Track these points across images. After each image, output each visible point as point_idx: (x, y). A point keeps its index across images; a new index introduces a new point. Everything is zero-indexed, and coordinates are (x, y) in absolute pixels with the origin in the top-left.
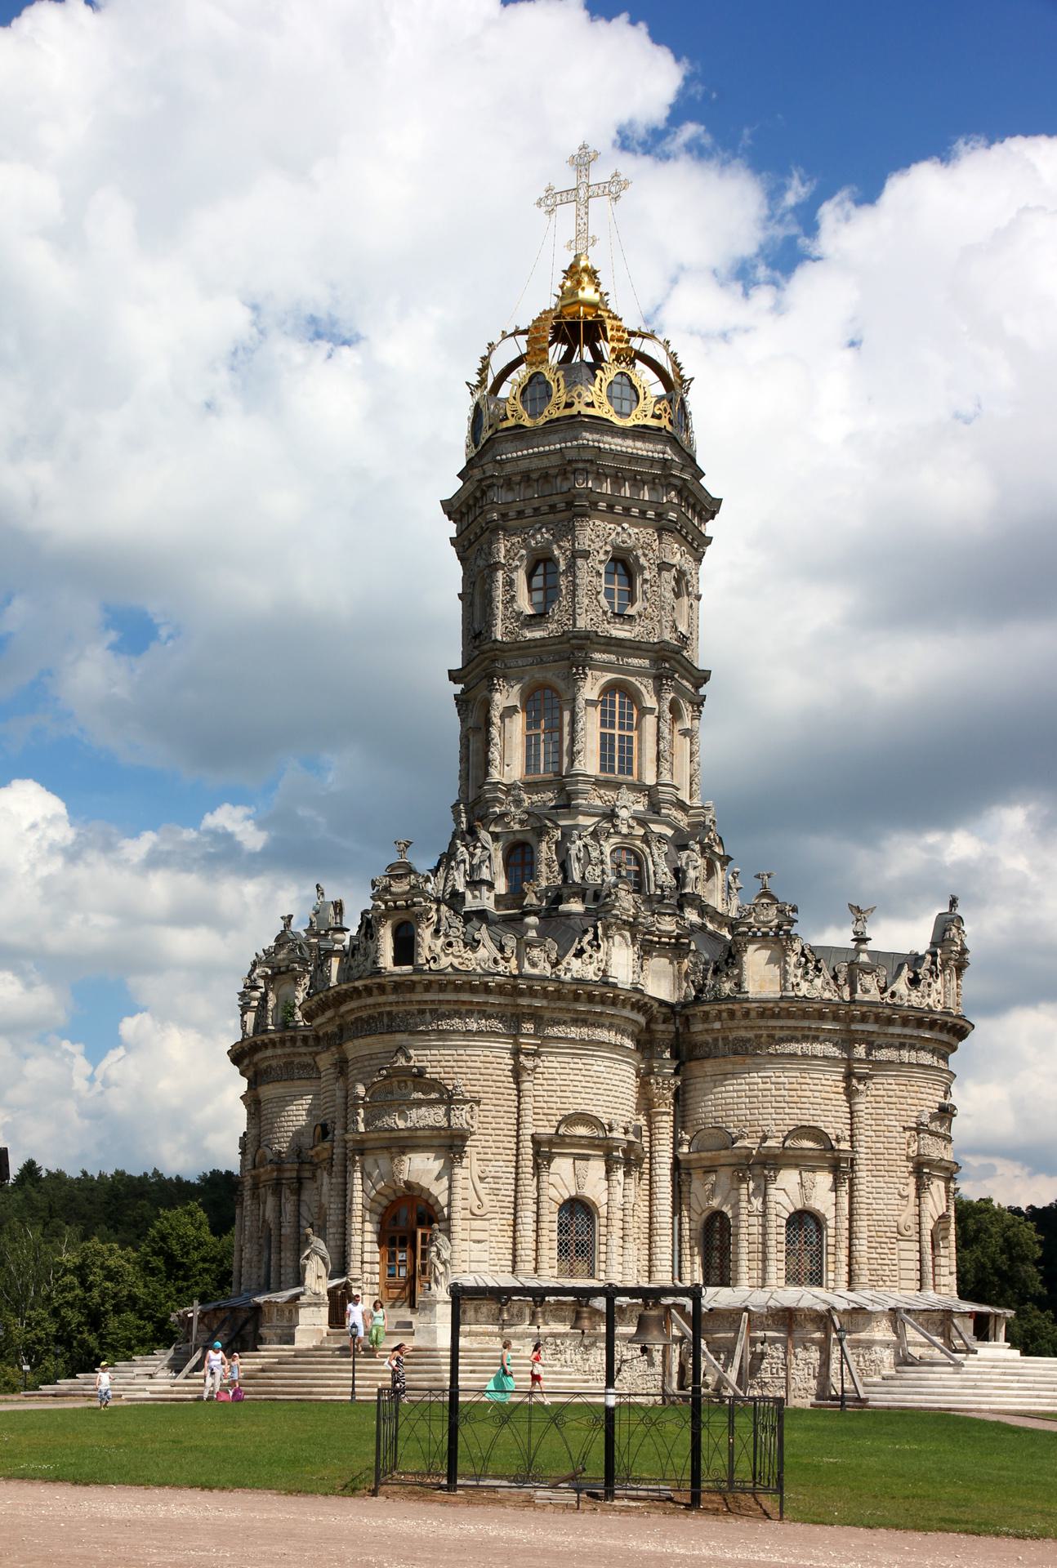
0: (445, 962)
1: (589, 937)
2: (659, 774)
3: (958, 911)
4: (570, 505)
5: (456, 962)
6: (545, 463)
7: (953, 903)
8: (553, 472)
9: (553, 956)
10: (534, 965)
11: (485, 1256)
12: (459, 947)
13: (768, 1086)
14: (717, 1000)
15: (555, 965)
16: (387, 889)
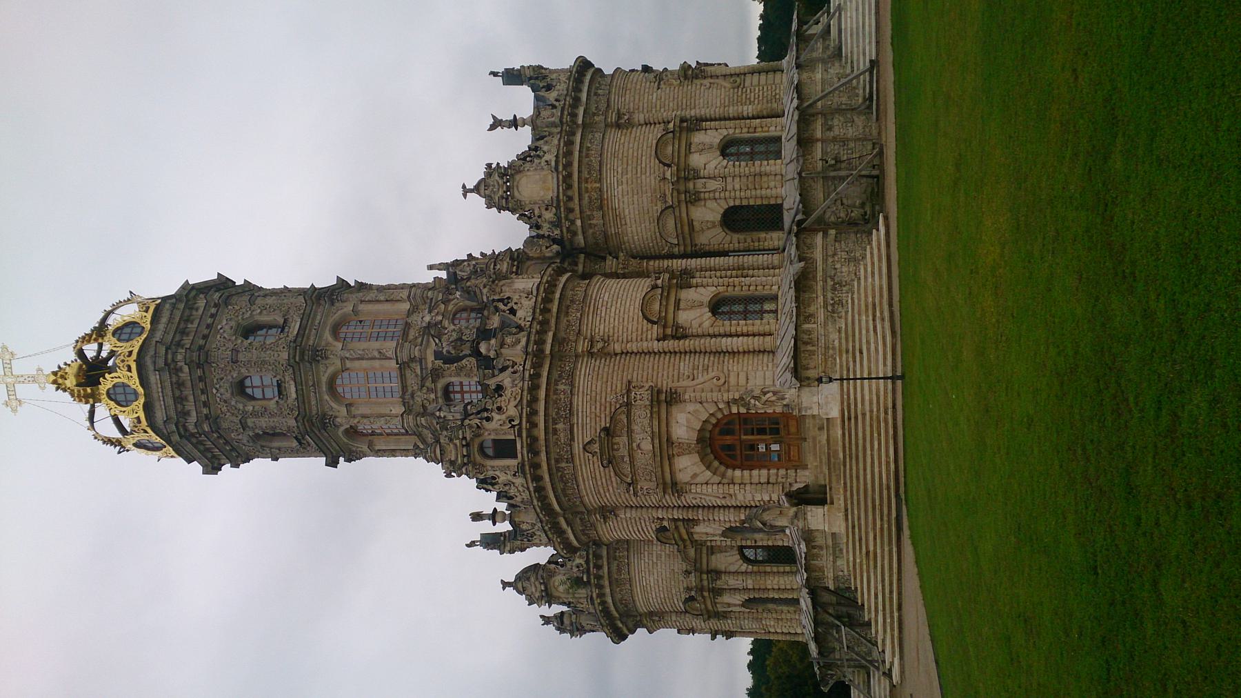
0: (512, 411)
1: (501, 306)
3: (501, 70)
4: (199, 366)
5: (513, 403)
6: (168, 384)
7: (495, 74)
8: (174, 380)
9: (514, 330)
10: (519, 341)
11: (760, 374)
12: (501, 401)
13: (624, 180)
14: (557, 224)
15: (520, 328)
16: (452, 463)
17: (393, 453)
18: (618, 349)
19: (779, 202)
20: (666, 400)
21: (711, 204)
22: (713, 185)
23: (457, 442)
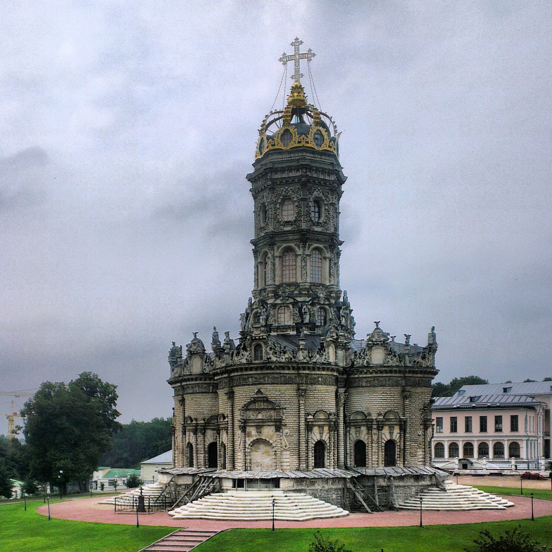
2: (330, 281)
17: (256, 273)
18: (301, 402)
19: (367, 465)
20: (279, 426)
21: (366, 437)
22: (375, 438)
23: (262, 334)
